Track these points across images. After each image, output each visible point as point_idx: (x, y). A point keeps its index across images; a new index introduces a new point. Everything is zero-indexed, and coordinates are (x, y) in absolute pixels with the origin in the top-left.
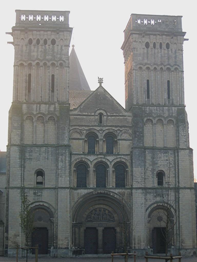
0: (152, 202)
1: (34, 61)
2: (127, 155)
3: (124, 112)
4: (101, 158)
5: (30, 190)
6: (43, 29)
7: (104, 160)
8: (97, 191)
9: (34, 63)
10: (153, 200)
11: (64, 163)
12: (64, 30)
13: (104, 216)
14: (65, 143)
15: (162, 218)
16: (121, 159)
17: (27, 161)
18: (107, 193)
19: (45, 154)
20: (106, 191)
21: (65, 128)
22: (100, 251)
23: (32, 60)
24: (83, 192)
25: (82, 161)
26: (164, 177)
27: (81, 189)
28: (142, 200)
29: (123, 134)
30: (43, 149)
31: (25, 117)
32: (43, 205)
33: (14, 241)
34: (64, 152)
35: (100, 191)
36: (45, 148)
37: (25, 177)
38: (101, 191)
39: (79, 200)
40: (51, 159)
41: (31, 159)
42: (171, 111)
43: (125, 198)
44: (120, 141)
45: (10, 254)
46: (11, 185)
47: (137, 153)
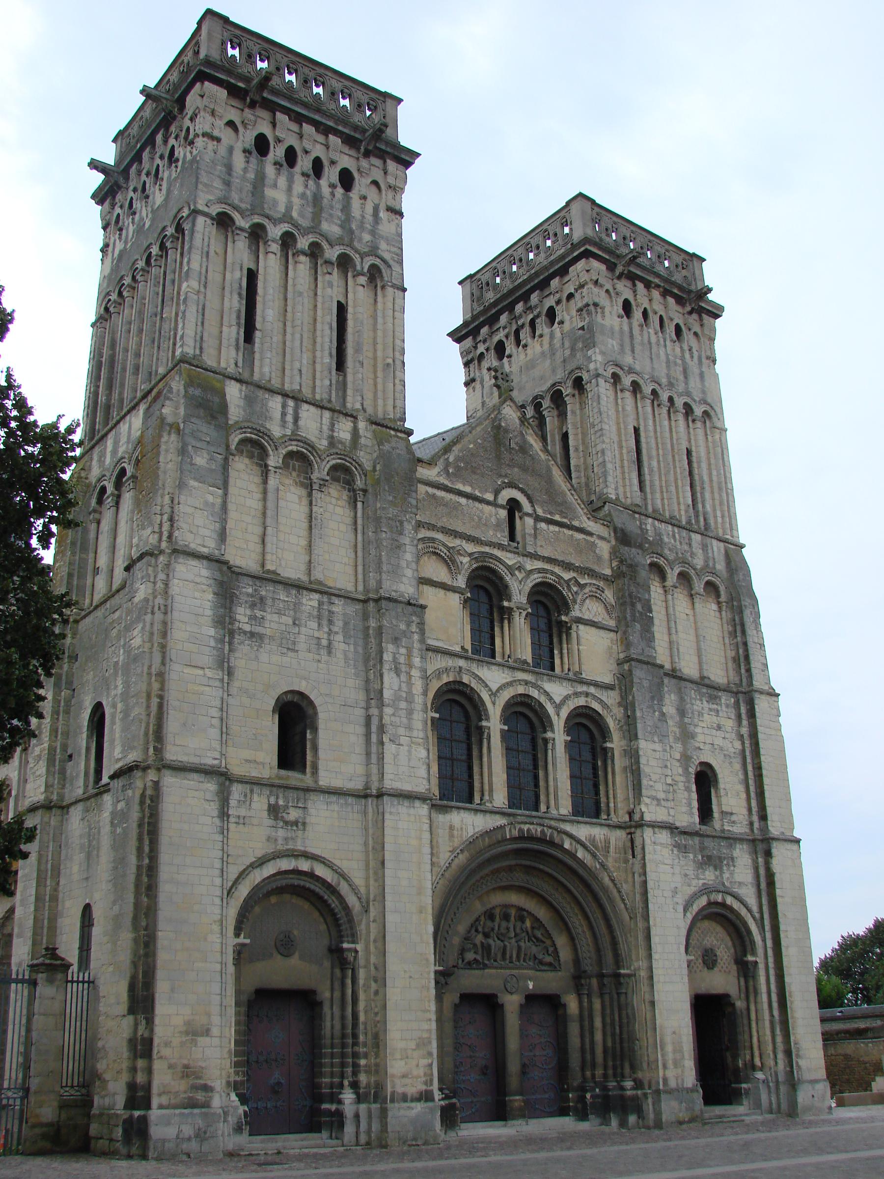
1: (276, 222)
2: (609, 687)
3: (586, 519)
4: (527, 683)
5: (252, 791)
6: (317, 117)
7: (535, 693)
8: (518, 826)
9: (275, 232)
10: (696, 881)
11: (403, 677)
12: (388, 150)
14: (402, 588)
15: (716, 955)
16: (589, 700)
17: (242, 643)
18: (551, 836)
19: (319, 625)
20: (550, 827)
21: (401, 523)
22: (516, 1104)
23: (268, 217)
25: (461, 683)
26: (713, 791)
27: (462, 811)
28: (673, 874)
29: (587, 601)
30: (310, 599)
31: (235, 439)
32: (311, 875)
33: (186, 1062)
36: (316, 596)
38: (531, 827)
39: (456, 861)
40: (345, 651)
41: (260, 637)
43: (610, 863)
45: (164, 1141)
46: (172, 754)
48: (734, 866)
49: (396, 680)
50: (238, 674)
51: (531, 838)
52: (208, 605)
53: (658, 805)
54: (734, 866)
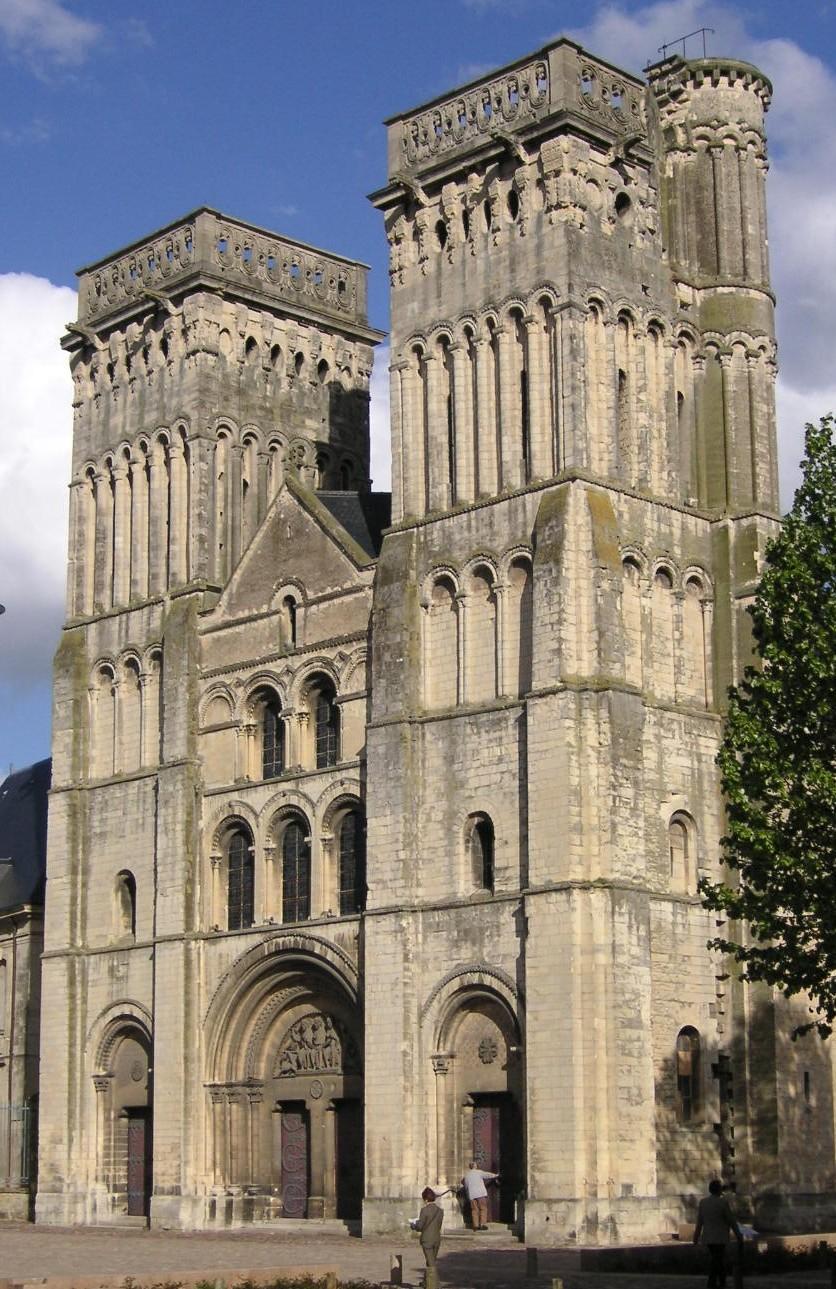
0: (444, 973)
11: (170, 835)
21: (176, 689)
24: (237, 947)
34: (171, 789)
37: (90, 912)
42: (520, 519)
44: (345, 705)
47: (381, 750)
48: (499, 936)
49: (165, 839)
50: (95, 870)
51: (287, 951)
52: (65, 826)
53: (384, 888)
54: (499, 936)
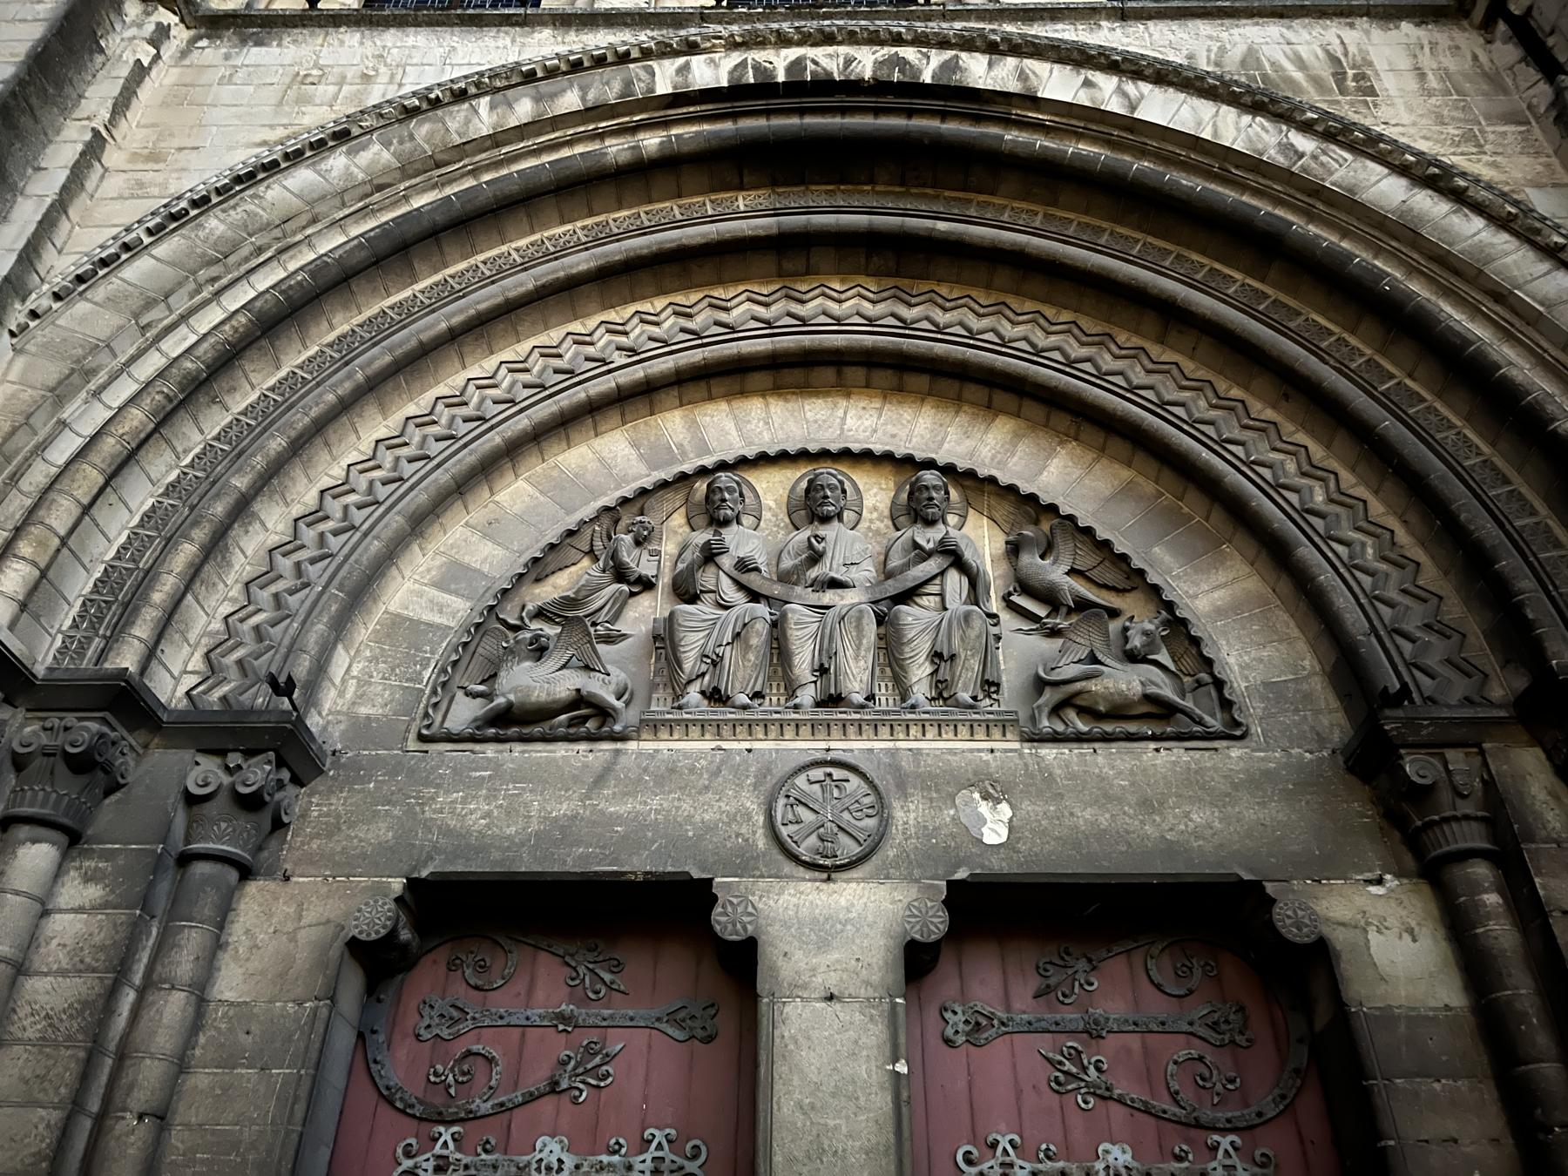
13: (916, 618)
18: (951, 66)
35: (793, 53)
39: (302, 178)
